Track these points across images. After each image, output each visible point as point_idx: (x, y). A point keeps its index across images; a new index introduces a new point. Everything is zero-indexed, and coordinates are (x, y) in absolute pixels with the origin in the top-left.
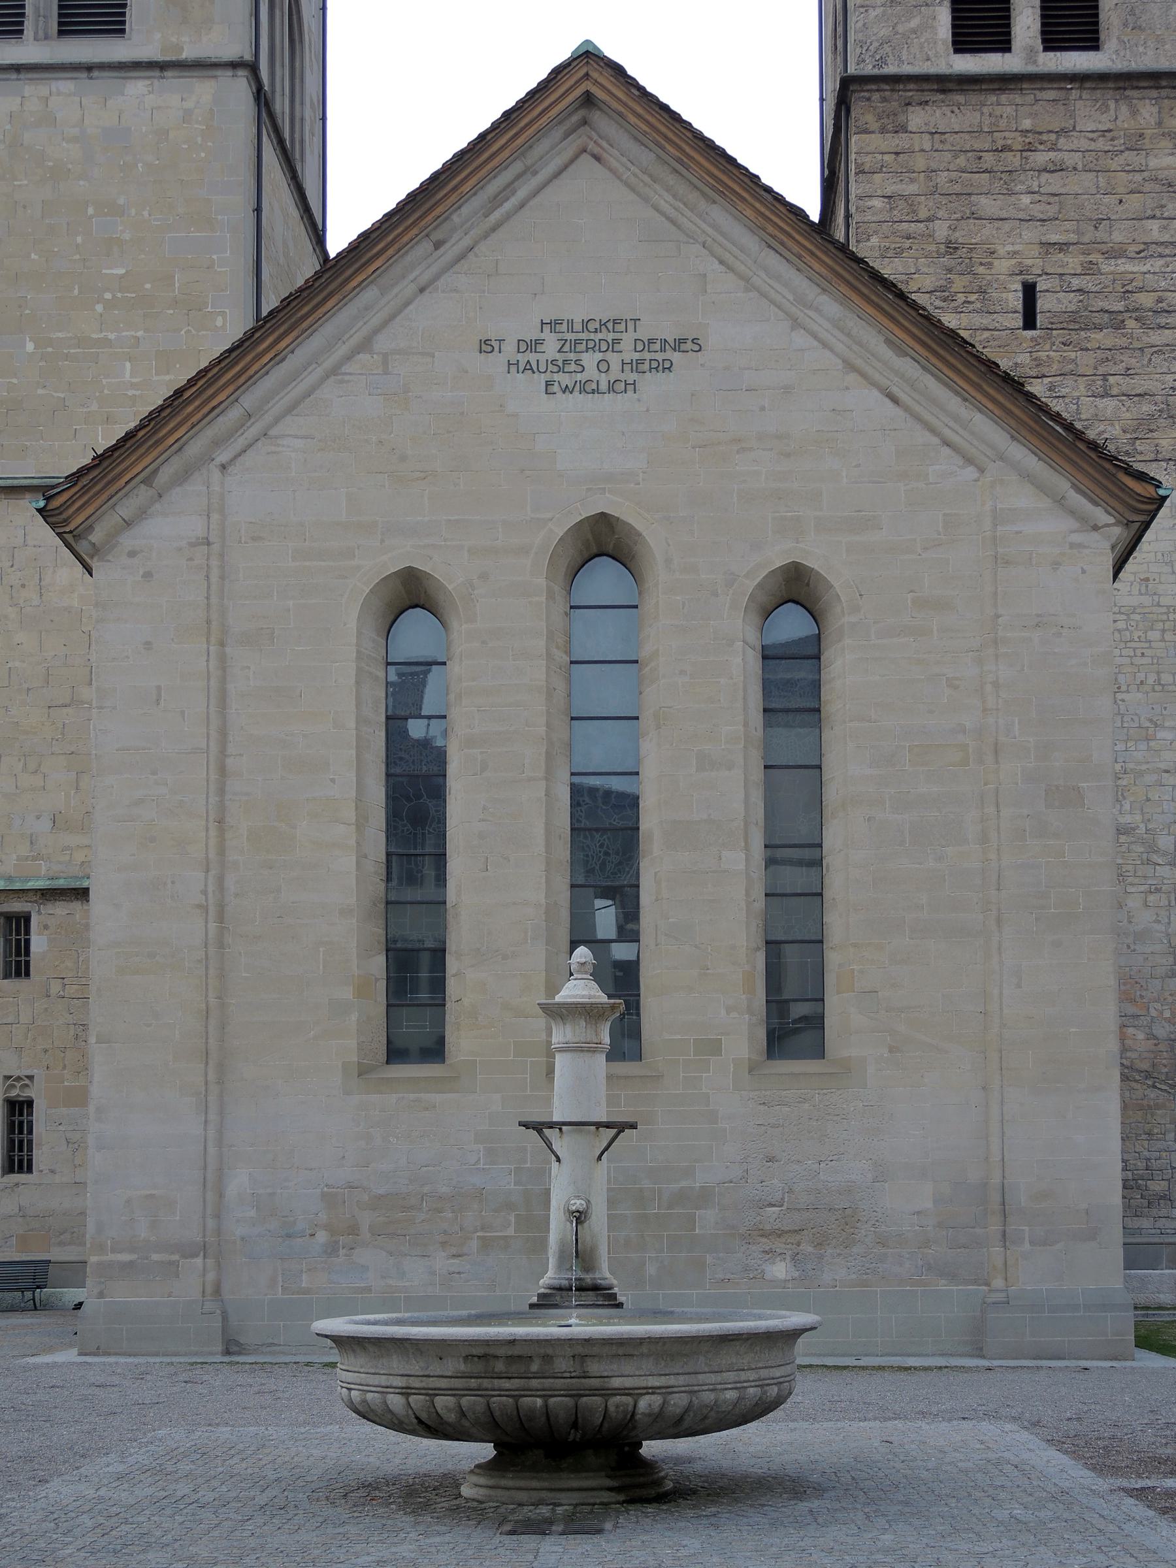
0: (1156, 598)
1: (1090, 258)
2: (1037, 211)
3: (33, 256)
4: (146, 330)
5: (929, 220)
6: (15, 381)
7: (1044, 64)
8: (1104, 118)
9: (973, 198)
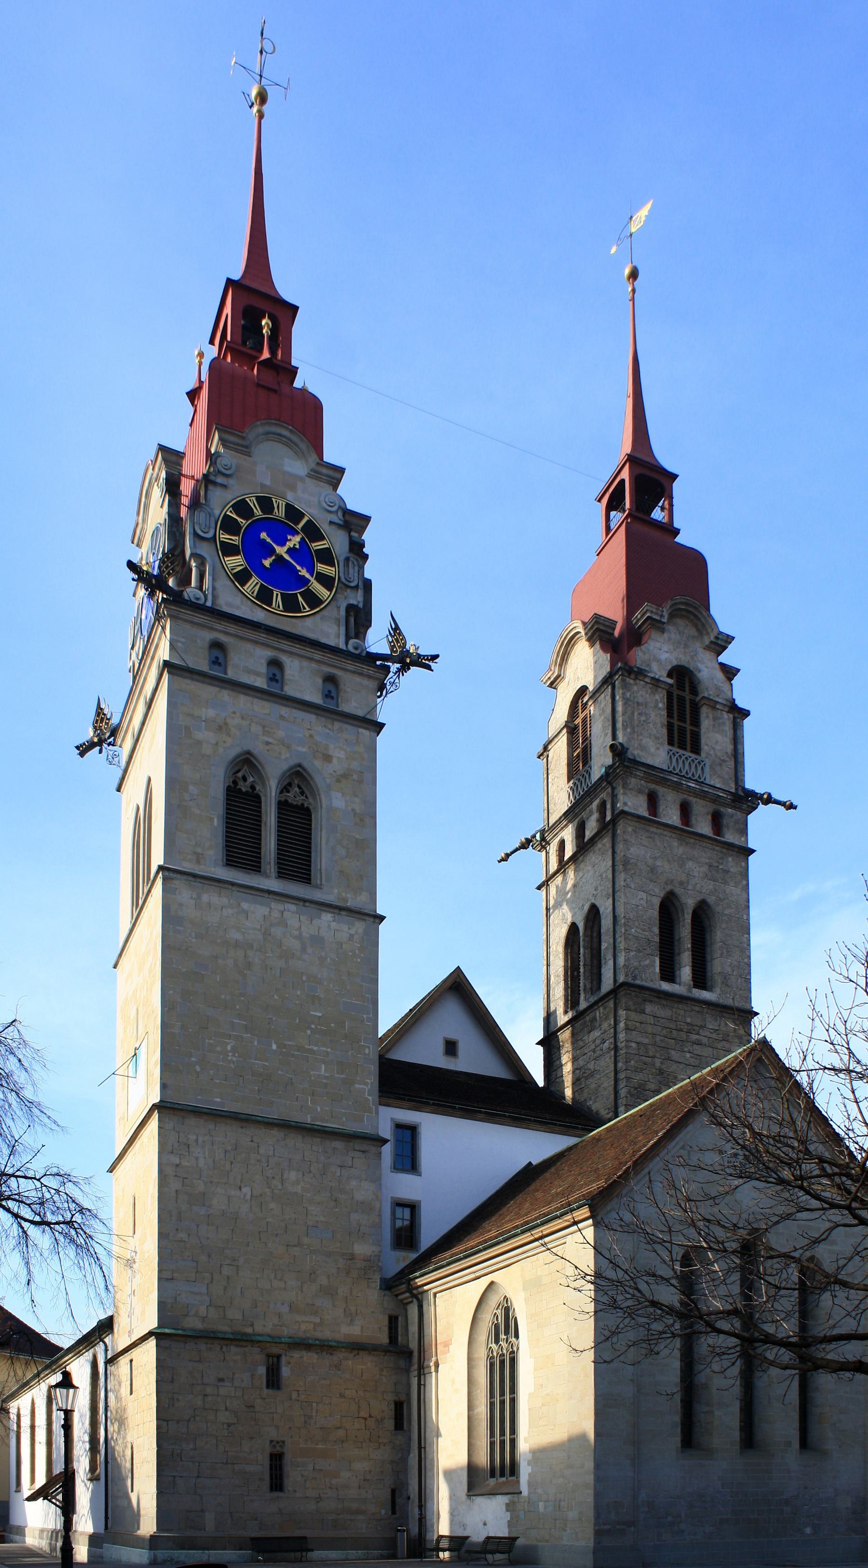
3: (276, 997)
4: (332, 1049)
6: (267, 1064)
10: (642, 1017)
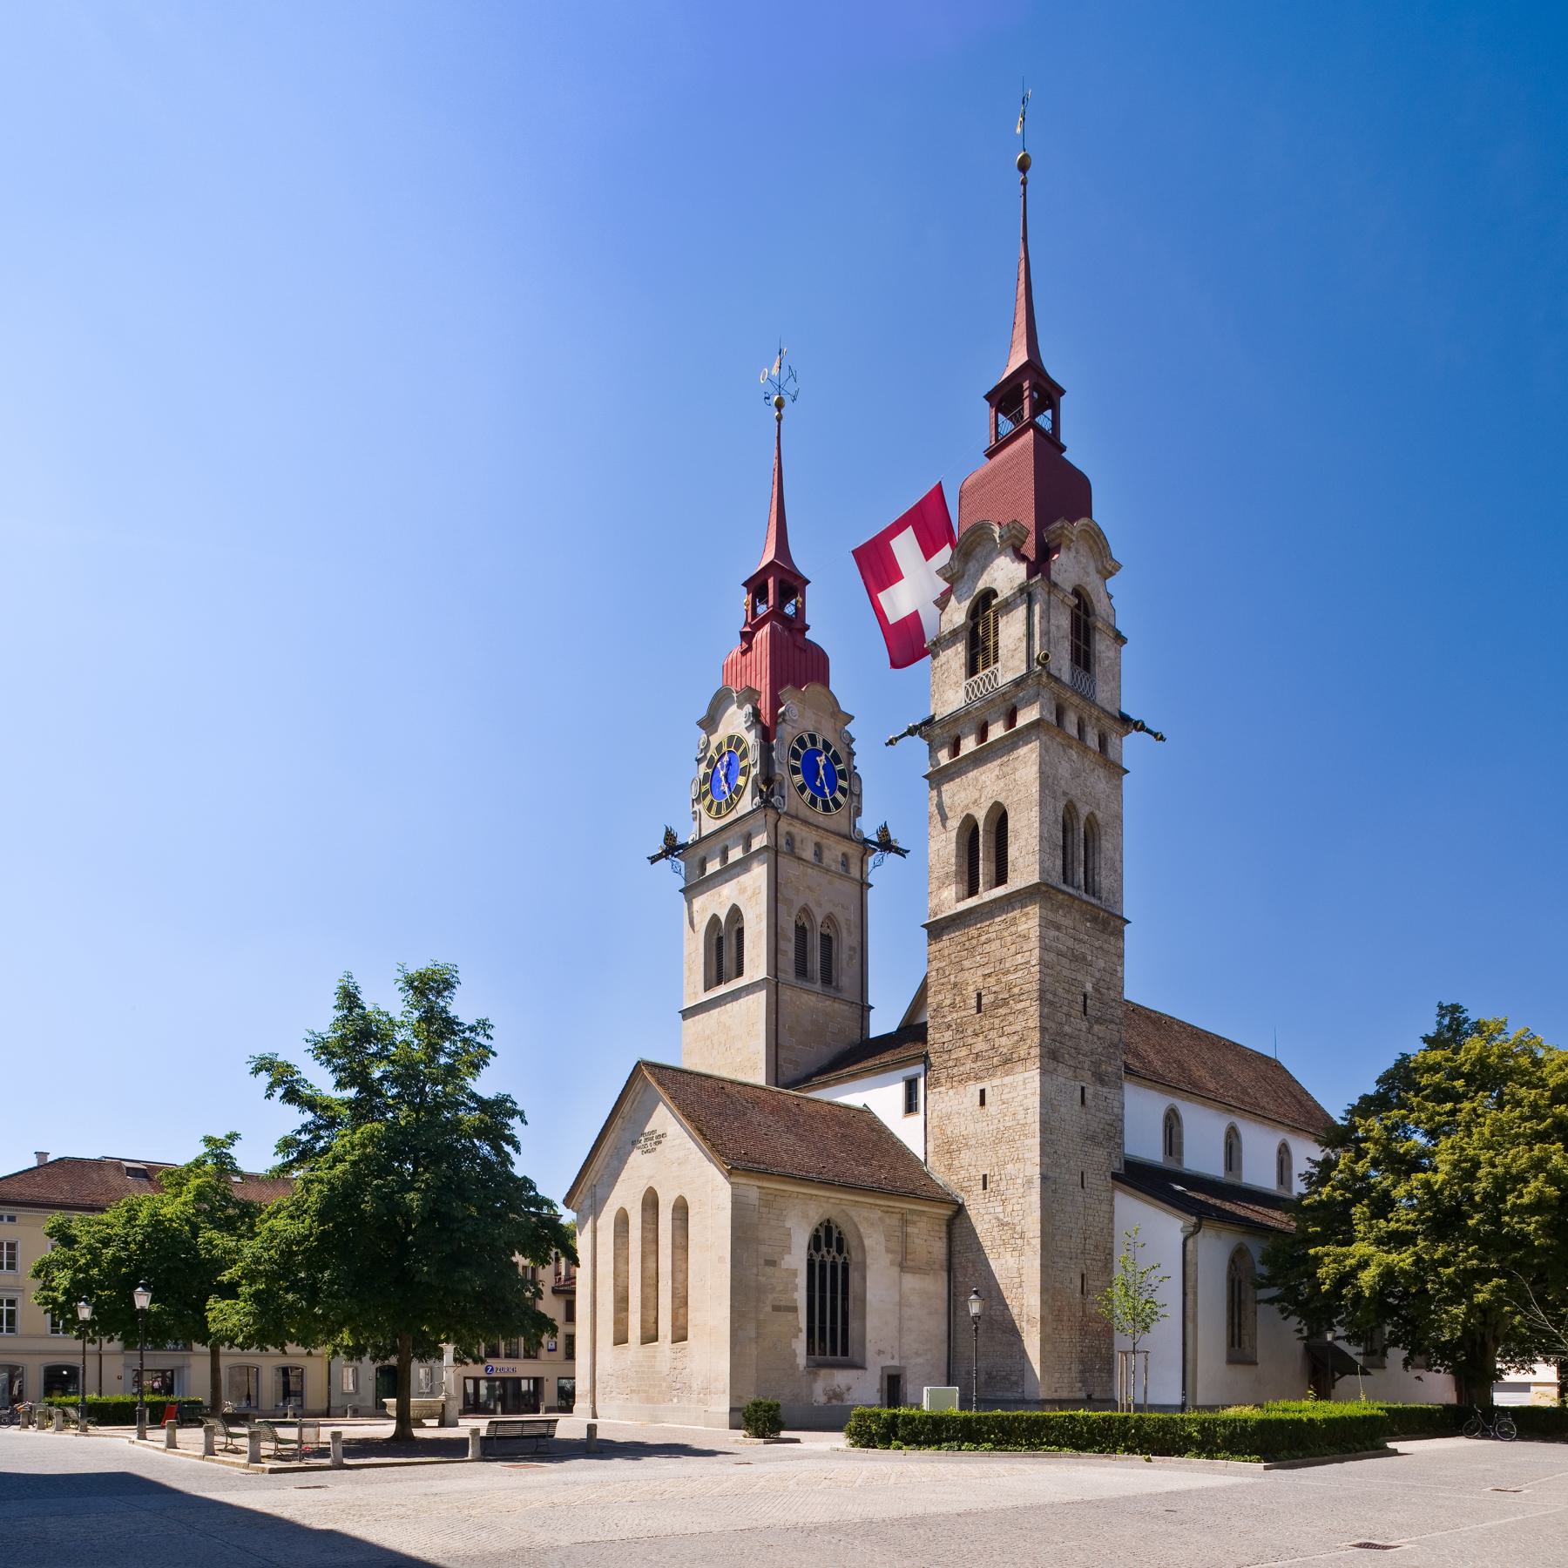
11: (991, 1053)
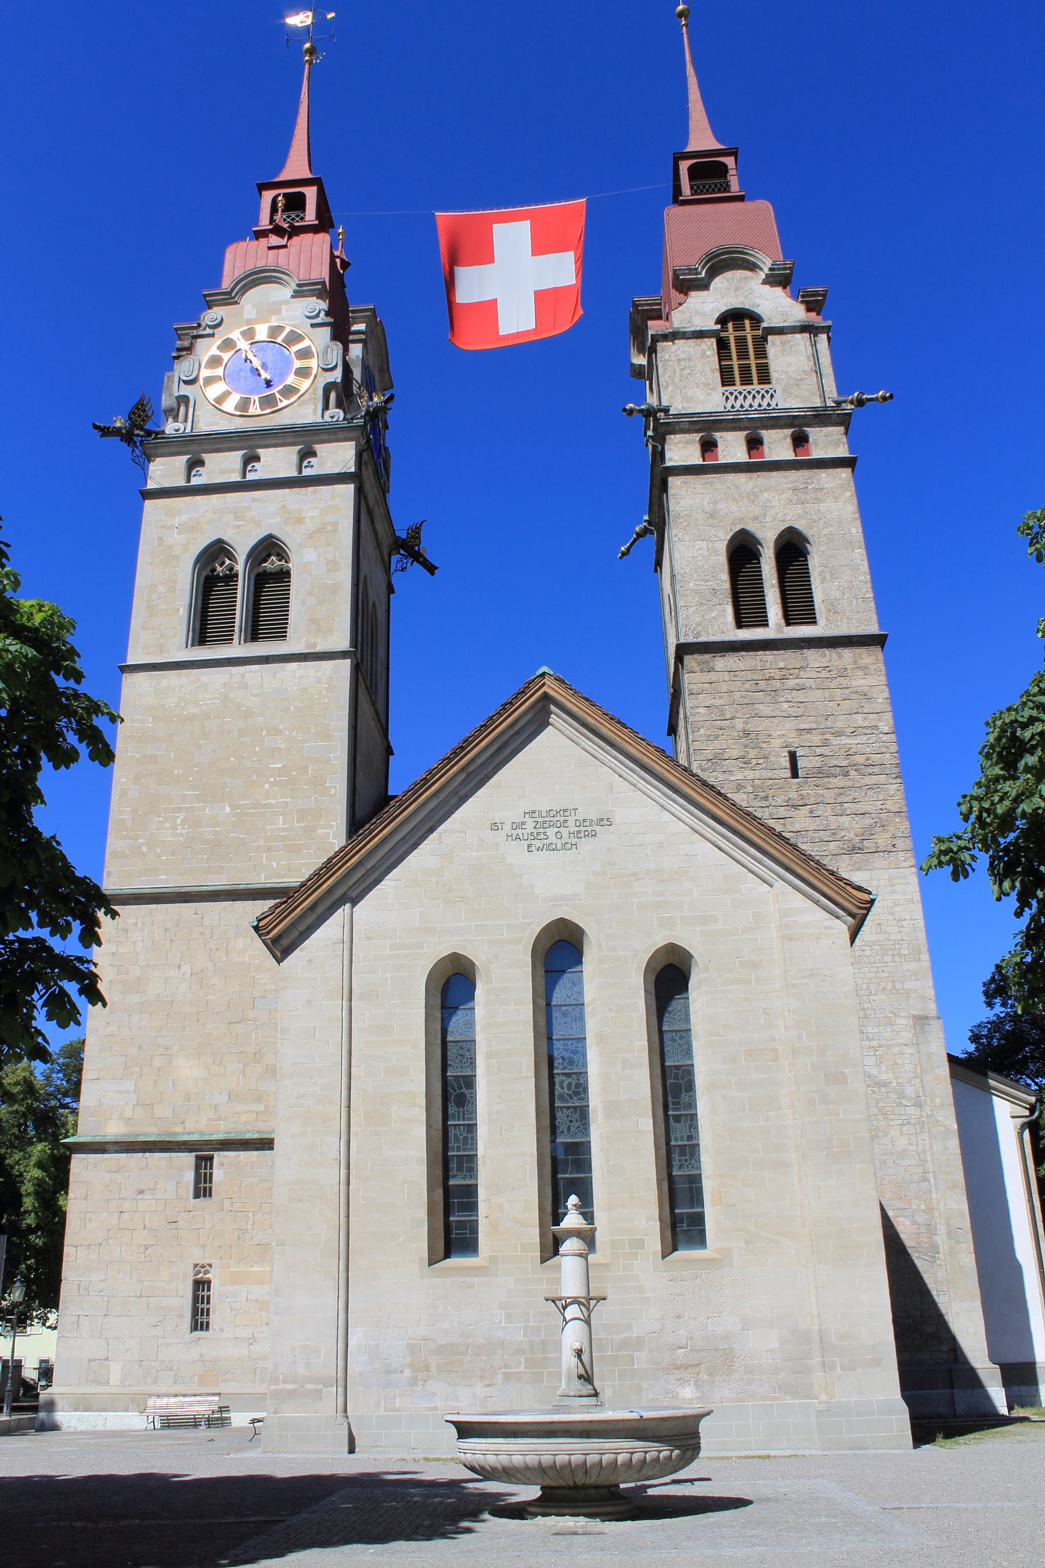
0: (886, 935)
1: (826, 736)
2: (792, 711)
3: (232, 759)
4: (292, 798)
5: (732, 719)
6: (218, 829)
7: (787, 633)
8: (824, 660)
9: (755, 706)
10: (712, 676)
11: (825, 835)
